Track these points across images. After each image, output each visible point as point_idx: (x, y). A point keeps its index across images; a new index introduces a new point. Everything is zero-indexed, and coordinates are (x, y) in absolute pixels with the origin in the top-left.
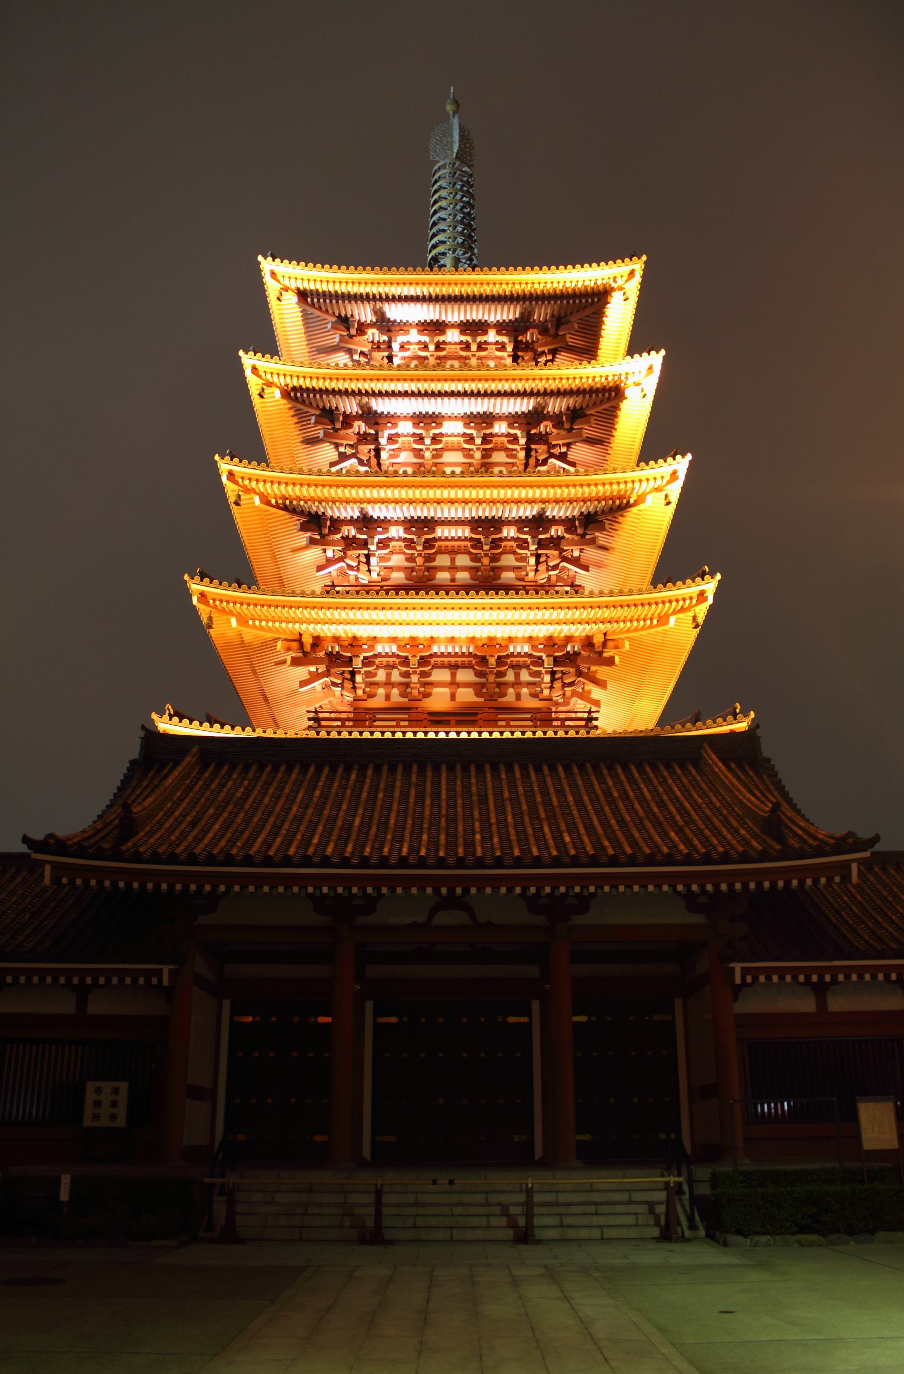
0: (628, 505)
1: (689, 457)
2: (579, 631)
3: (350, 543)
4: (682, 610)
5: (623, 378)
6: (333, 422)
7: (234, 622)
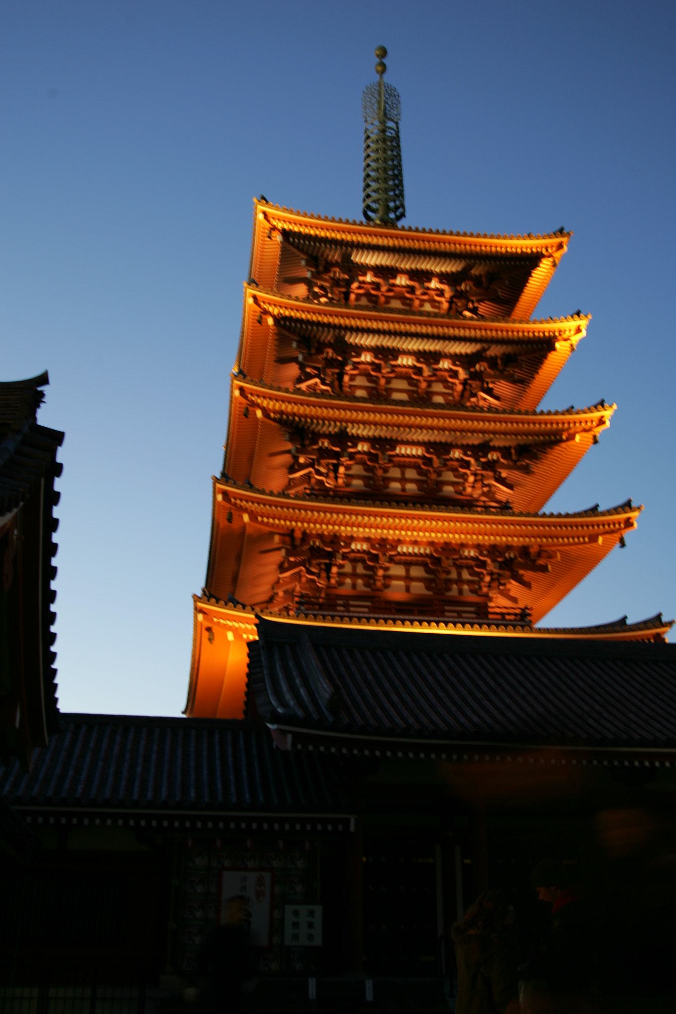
0: (562, 441)
2: (515, 541)
3: (324, 453)
4: (612, 532)
5: (557, 334)
6: (309, 348)
7: (246, 518)
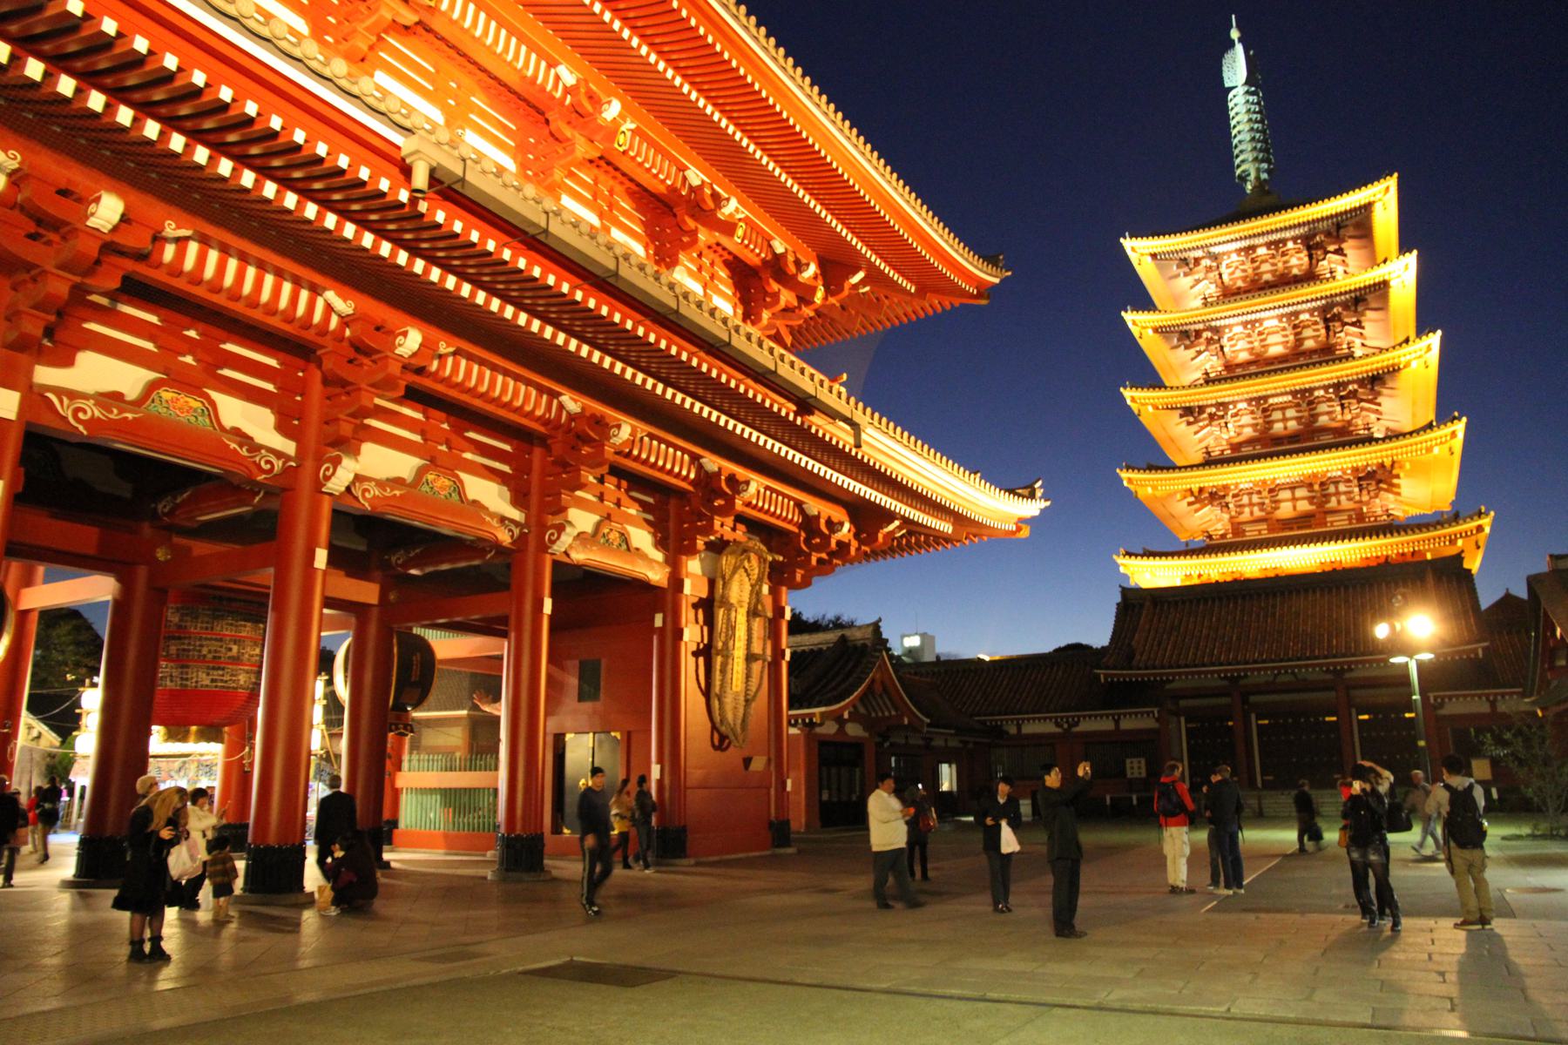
1: (1439, 332)
3: (1212, 417)
7: (1150, 490)
